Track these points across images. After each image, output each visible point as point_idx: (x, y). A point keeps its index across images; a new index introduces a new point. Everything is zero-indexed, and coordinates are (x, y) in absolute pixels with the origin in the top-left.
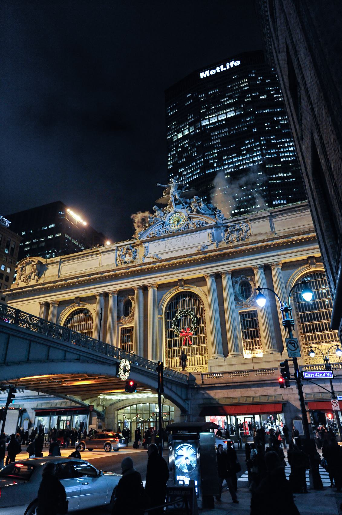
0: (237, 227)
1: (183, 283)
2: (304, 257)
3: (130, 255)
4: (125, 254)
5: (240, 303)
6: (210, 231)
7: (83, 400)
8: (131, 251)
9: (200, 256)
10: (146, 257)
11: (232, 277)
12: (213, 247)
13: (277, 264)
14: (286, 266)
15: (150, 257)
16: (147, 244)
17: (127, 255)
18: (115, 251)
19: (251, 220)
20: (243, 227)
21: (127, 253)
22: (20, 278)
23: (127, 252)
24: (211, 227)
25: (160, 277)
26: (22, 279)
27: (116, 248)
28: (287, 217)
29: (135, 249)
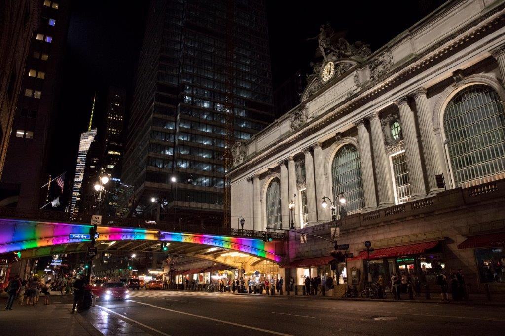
0: (381, 59)
1: (339, 137)
2: (448, 74)
4: (295, 119)
5: (389, 147)
6: (354, 73)
9: (346, 104)
10: (309, 117)
11: (380, 119)
12: (359, 90)
13: (420, 91)
14: (432, 91)
16: (308, 105)
17: (297, 120)
19: (392, 47)
20: (386, 57)
24: (355, 69)
27: (288, 115)
28: (429, 29)
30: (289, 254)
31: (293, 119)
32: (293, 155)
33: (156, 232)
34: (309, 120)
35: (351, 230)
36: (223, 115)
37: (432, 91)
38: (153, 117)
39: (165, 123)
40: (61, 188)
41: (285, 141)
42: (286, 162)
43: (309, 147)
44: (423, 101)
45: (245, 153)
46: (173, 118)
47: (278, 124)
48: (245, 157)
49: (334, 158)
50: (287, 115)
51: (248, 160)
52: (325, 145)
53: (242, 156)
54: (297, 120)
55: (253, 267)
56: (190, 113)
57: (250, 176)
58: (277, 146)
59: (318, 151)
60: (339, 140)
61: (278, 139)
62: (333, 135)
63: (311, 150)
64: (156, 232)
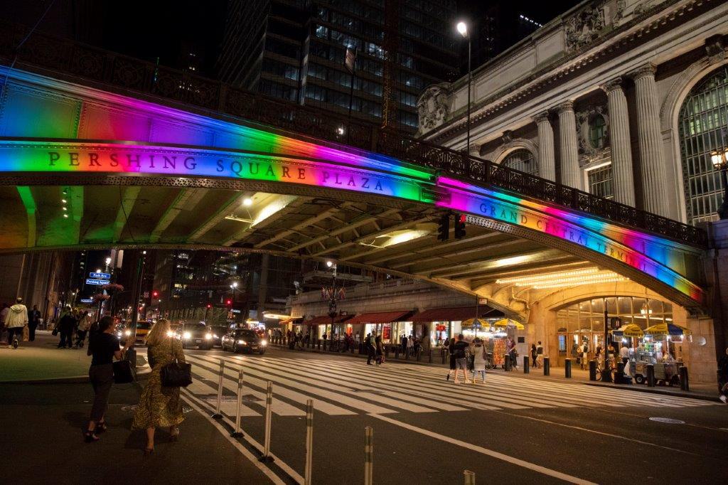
1: (718, 44)
3: (590, 25)
4: (580, 28)
7: (473, 288)
8: (590, 16)
10: (624, 15)
15: (632, 13)
17: (585, 27)
18: (562, 28)
21: (583, 24)
22: (423, 123)
23: (583, 23)
25: (657, 47)
26: (425, 124)
27: (561, 21)
29: (600, 11)
31: (573, 28)
32: (573, 99)
33: (426, 175)
34: (622, 22)
36: (377, 63)
37: (663, 71)
38: (264, 57)
39: (282, 68)
41: (555, 72)
42: (553, 116)
43: (622, 76)
44: (649, 88)
45: (447, 107)
46: (295, 62)
47: (533, 43)
48: (447, 115)
49: (688, 97)
50: (558, 20)
51: (453, 121)
52: (663, 71)
53: (441, 112)
54: (585, 27)
55: (552, 315)
56: (324, 55)
58: (534, 82)
60: (508, 141)
61: (533, 70)
62: (700, 42)
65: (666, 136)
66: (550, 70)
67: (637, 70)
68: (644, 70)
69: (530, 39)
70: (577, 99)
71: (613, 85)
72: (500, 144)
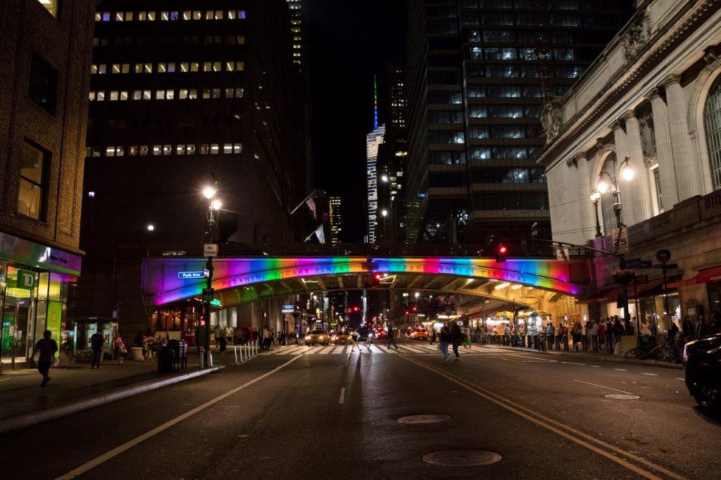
1: (711, 55)
4: (631, 43)
10: (652, 32)
16: (648, 9)
17: (635, 43)
18: (621, 44)
21: (632, 39)
30: (595, 281)
31: (628, 43)
32: (633, 107)
33: (365, 260)
35: (684, 231)
36: (537, 65)
38: (428, 91)
39: (448, 96)
40: (312, 211)
41: (615, 87)
42: (622, 123)
45: (560, 119)
46: (457, 87)
47: (605, 59)
48: (561, 126)
49: (707, 98)
50: (617, 38)
51: (568, 127)
52: (687, 77)
53: (557, 125)
54: (635, 43)
55: (553, 305)
56: (482, 74)
57: (571, 155)
58: (604, 97)
59: (675, 90)
62: (700, 54)
63: (661, 91)
64: (365, 260)
65: (692, 136)
66: (611, 87)
67: (663, 82)
68: (669, 81)
69: (602, 55)
70: (636, 107)
71: (652, 95)
72: (597, 150)
